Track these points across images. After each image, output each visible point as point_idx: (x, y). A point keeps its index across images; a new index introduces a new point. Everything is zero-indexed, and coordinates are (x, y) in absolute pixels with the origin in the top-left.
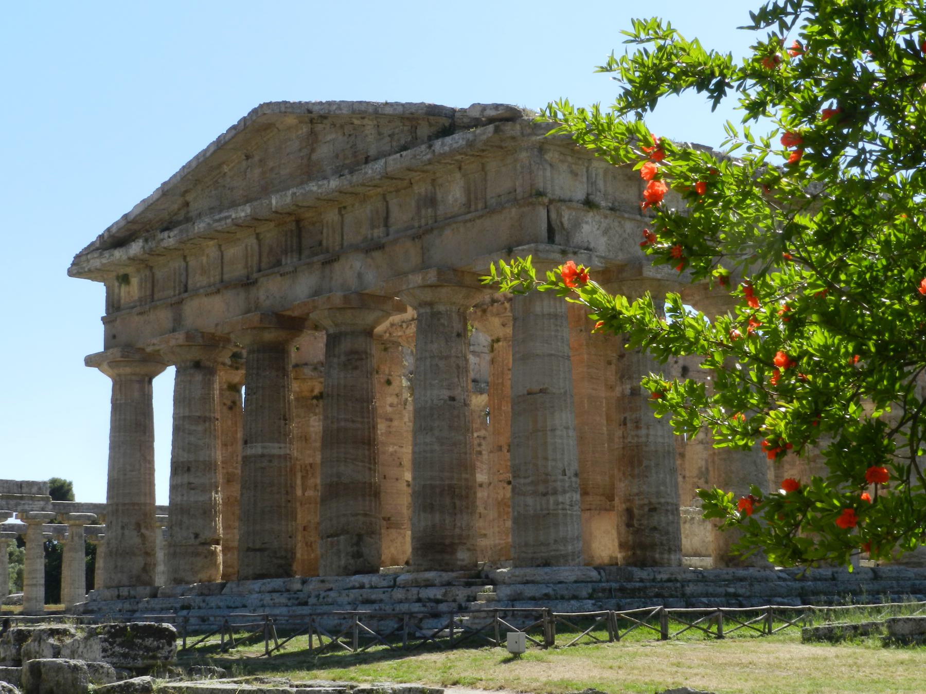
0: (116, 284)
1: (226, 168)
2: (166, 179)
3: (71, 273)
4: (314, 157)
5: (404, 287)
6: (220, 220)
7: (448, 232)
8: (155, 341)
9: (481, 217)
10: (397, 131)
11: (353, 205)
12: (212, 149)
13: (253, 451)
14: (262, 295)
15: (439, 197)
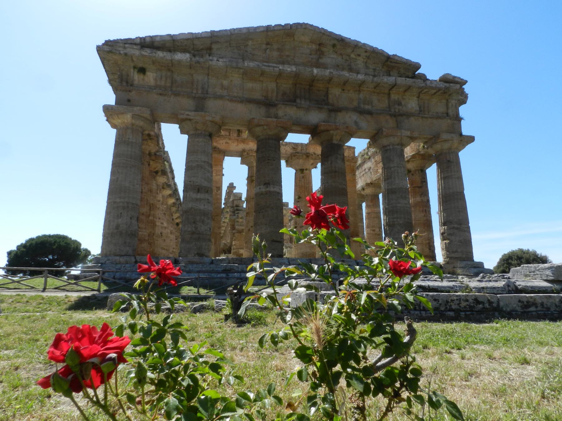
0: (132, 70)
1: (250, 43)
2: (217, 29)
3: (99, 49)
4: (321, 61)
5: (399, 134)
6: (269, 66)
7: (412, 119)
8: (190, 113)
9: (431, 118)
10: (378, 69)
11: (349, 91)
12: (262, 29)
13: (275, 189)
14: (280, 113)
15: (403, 103)
